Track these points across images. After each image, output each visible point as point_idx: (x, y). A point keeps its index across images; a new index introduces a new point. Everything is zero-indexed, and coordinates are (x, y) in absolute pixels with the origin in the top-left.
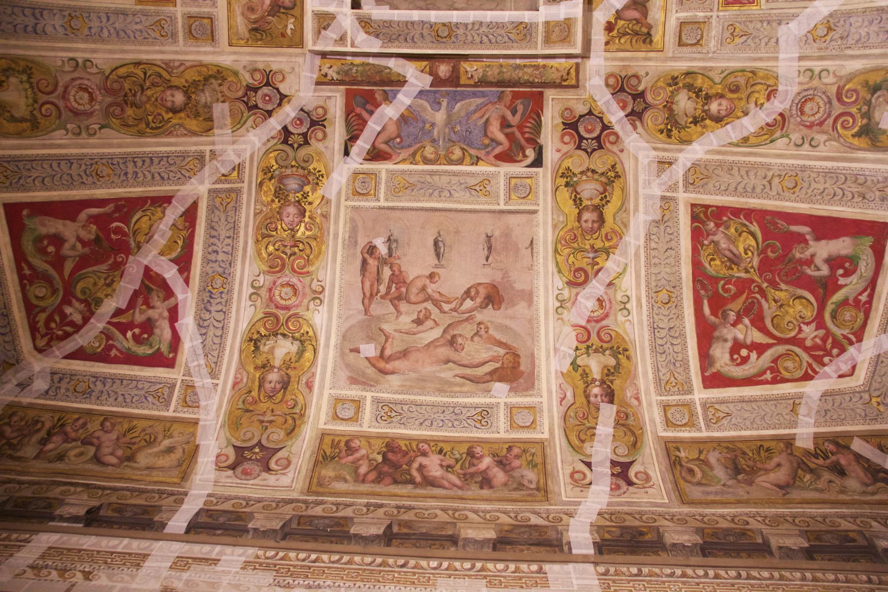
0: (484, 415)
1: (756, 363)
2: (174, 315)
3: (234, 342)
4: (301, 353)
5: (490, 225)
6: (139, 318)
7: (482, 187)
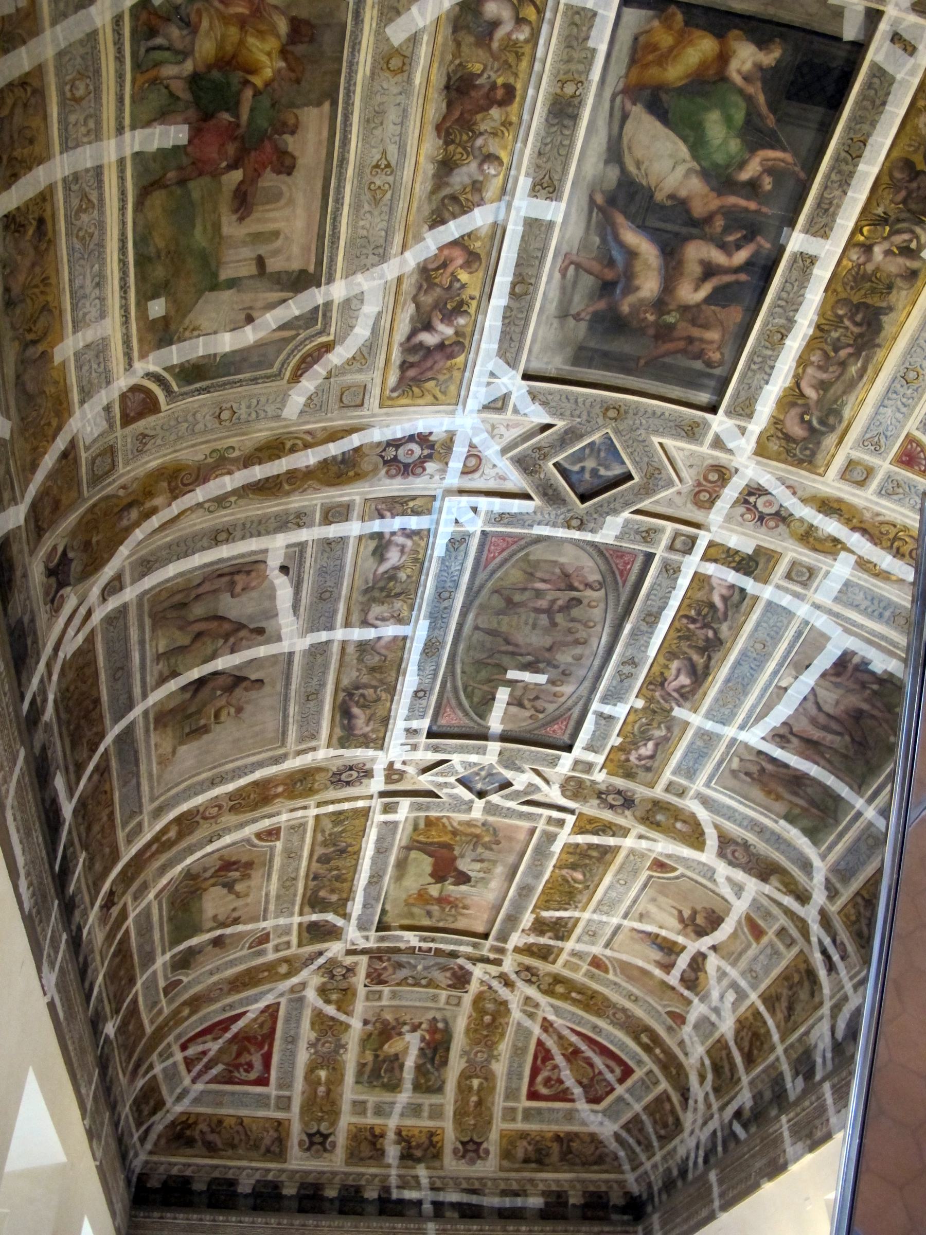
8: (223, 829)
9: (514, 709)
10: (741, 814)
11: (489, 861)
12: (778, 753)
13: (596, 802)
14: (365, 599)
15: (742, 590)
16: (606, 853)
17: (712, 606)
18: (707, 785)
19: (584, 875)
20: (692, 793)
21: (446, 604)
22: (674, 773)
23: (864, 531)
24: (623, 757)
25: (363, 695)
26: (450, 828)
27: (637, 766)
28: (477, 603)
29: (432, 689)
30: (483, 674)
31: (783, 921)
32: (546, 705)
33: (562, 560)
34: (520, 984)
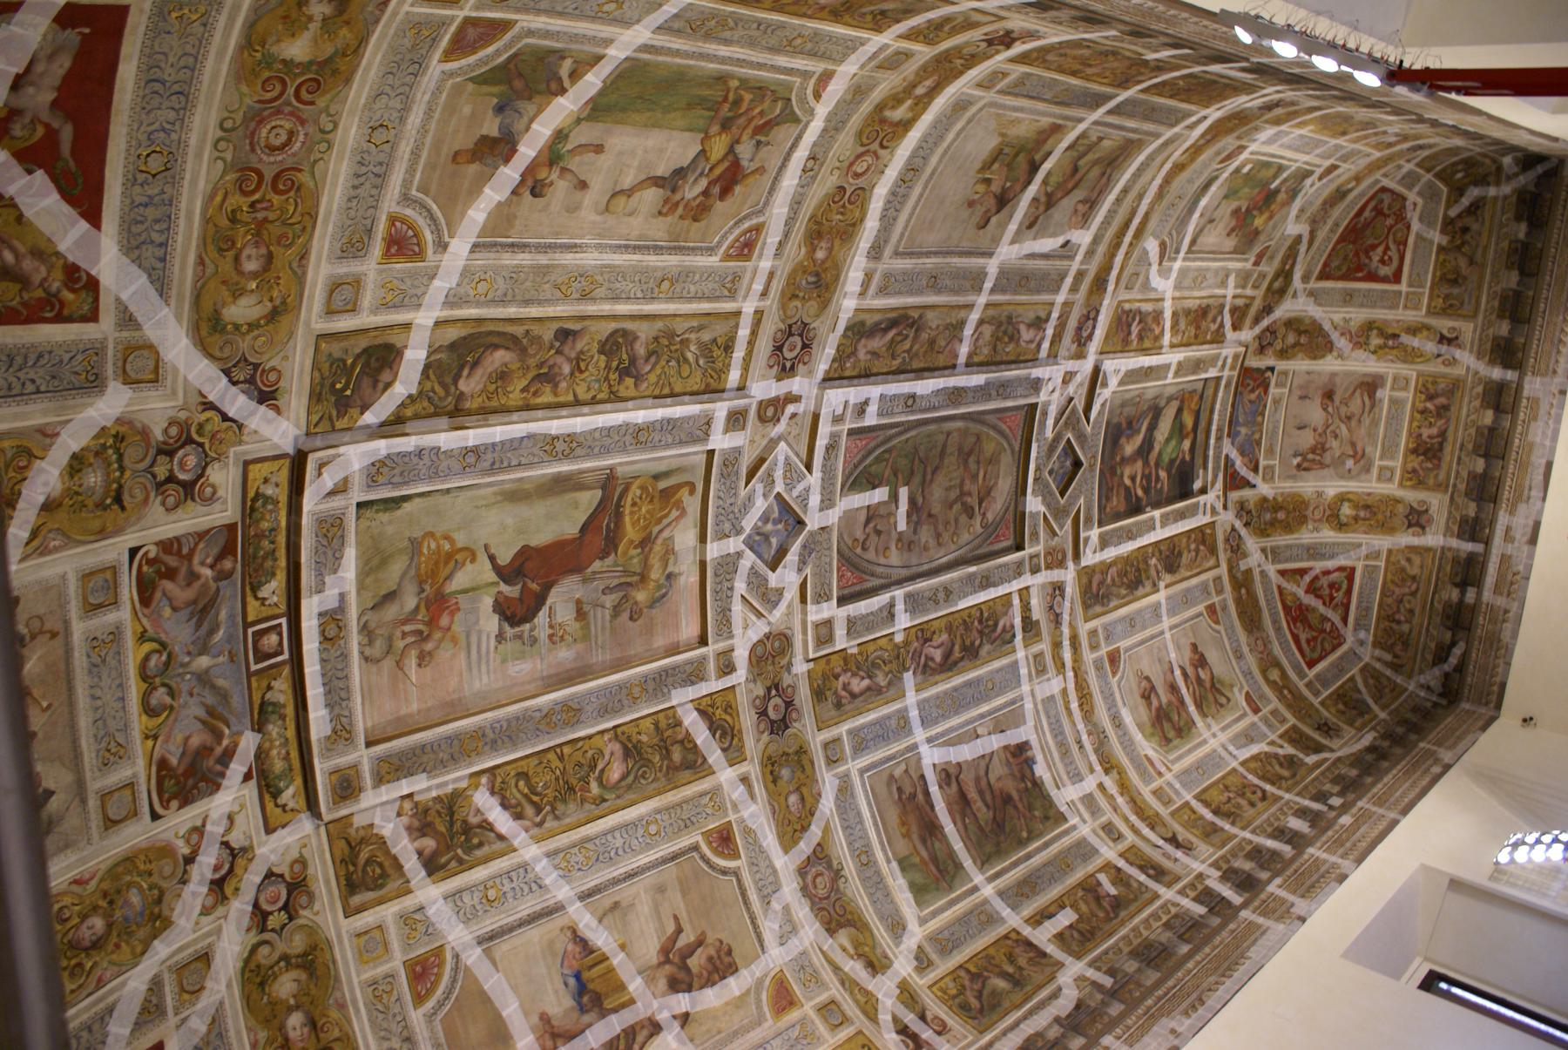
0: (1393, 401)
1: (1393, 253)
2: (1327, 573)
3: (1342, 537)
4: (1349, 500)
5: (1295, 398)
6: (1327, 592)
7: (1277, 402)
8: (814, 178)
9: (862, 517)
10: (864, 829)
11: (586, 627)
12: (934, 789)
13: (760, 690)
14: (1003, 319)
15: (1014, 636)
16: (695, 764)
17: (996, 625)
18: (862, 772)
19: (623, 778)
20: (842, 769)
21: (994, 393)
22: (850, 732)
23: (1076, 676)
24: (838, 670)
25: (906, 337)
26: (656, 530)
27: (836, 693)
28: (971, 425)
29: (912, 412)
30: (903, 463)
31: (835, 990)
32: (872, 550)
33: (1000, 482)
34: (240, 907)
